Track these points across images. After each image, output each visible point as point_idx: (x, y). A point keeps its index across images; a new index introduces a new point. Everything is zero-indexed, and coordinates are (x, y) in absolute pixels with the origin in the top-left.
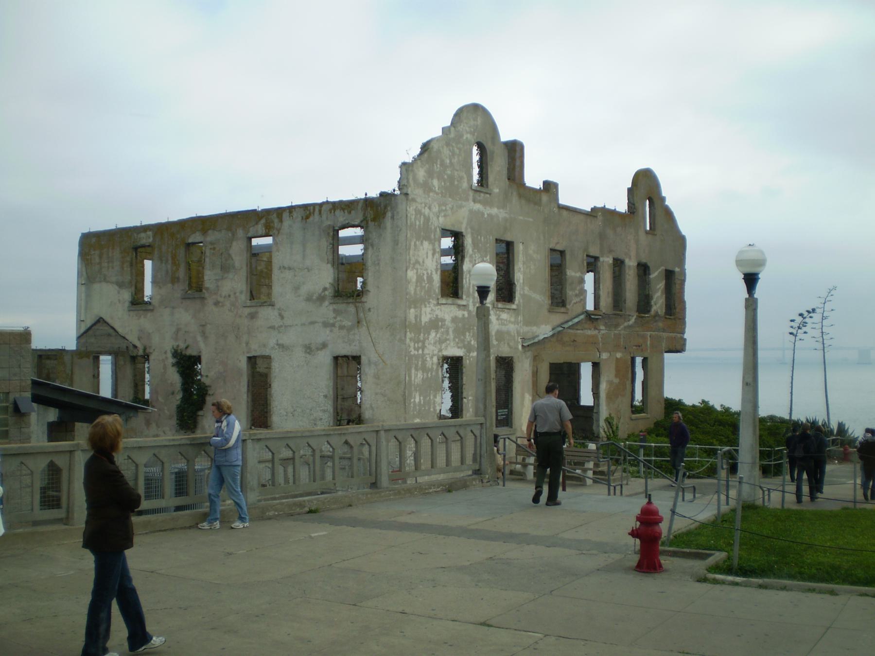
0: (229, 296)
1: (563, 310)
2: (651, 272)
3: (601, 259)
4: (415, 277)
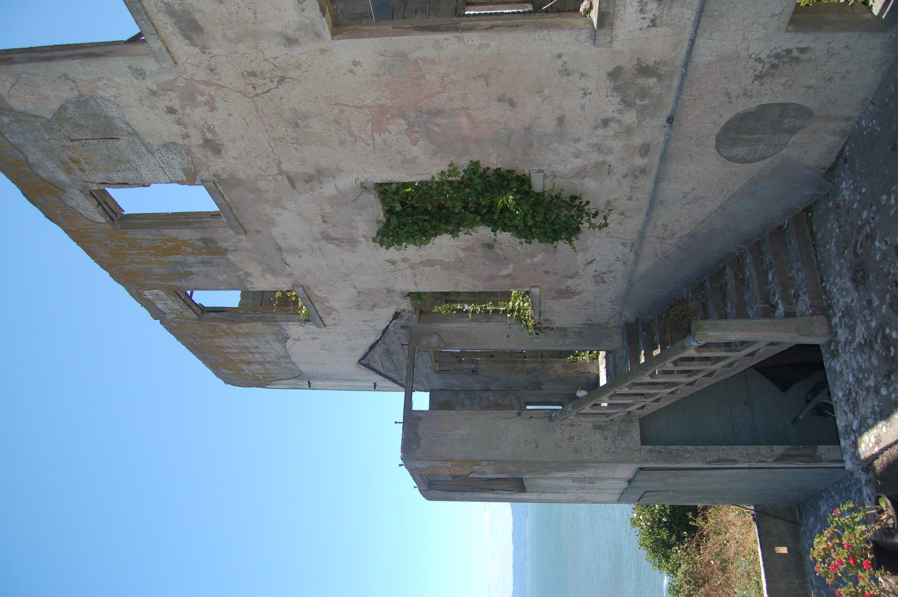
0: (171, 111)
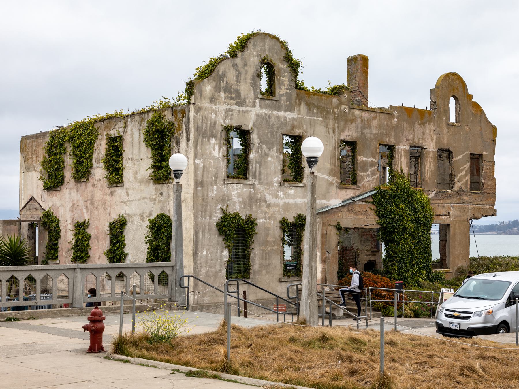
0: (100, 180)
1: (354, 187)
2: (454, 156)
3: (397, 147)
4: (202, 164)
